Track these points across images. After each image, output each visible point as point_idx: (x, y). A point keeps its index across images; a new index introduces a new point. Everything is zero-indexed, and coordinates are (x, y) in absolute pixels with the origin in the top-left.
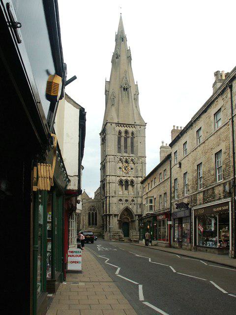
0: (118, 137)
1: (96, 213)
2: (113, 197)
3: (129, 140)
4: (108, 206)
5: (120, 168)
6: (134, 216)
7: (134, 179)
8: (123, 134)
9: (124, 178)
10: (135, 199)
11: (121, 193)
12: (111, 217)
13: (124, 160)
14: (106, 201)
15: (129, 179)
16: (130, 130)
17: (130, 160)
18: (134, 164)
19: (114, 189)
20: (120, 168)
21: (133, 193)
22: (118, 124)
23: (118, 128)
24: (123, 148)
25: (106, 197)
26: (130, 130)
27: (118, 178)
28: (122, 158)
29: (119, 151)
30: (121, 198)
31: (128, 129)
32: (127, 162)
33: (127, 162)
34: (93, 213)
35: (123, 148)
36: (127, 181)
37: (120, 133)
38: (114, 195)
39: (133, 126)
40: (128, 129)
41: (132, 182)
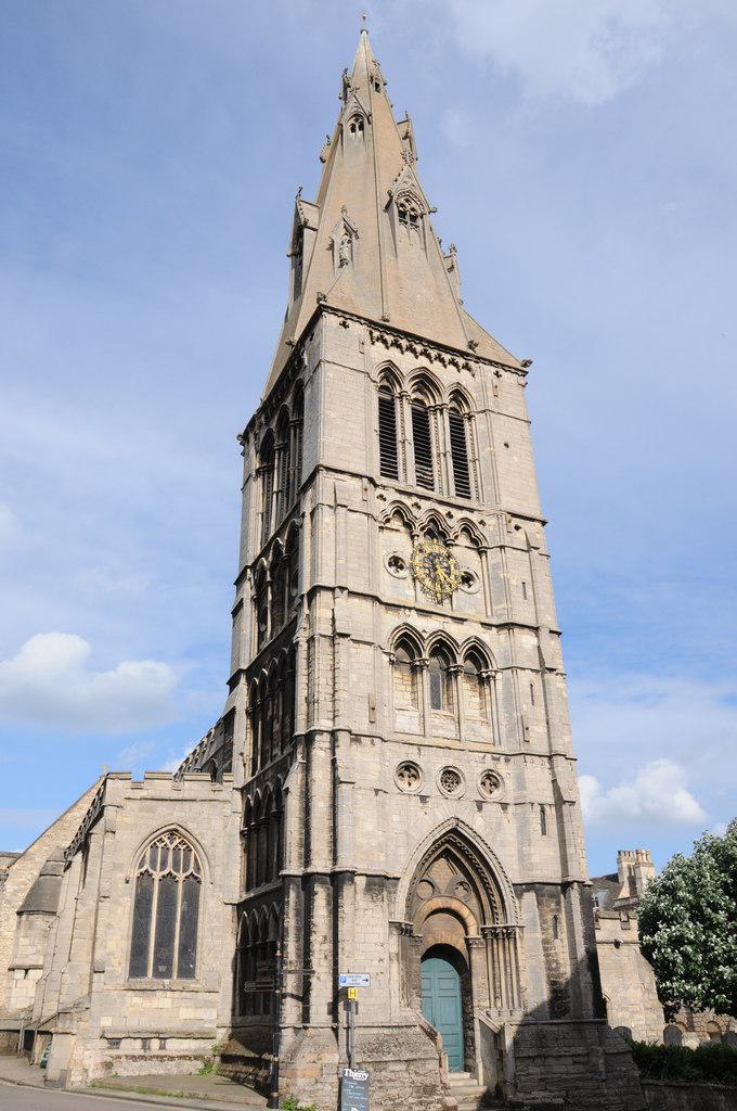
1: (194, 882)
2: (356, 738)
3: (440, 429)
4: (320, 806)
5: (396, 562)
7: (488, 637)
8: (408, 386)
10: (503, 769)
11: (407, 722)
12: (347, 891)
13: (421, 516)
14: (307, 768)
15: (459, 633)
16: (447, 376)
17: (454, 525)
18: (481, 552)
19: (365, 688)
20: (396, 562)
21: (485, 733)
22: (382, 330)
23: (380, 354)
24: (406, 453)
25: (309, 738)
26: (447, 376)
27: (392, 621)
28: (408, 501)
29: (389, 467)
30: (414, 758)
31: (436, 367)
32: (435, 530)
33: (435, 530)
35: (406, 453)
36: (443, 648)
37: (390, 374)
38: (362, 727)
39: (461, 361)
40: (436, 367)
41: (477, 654)
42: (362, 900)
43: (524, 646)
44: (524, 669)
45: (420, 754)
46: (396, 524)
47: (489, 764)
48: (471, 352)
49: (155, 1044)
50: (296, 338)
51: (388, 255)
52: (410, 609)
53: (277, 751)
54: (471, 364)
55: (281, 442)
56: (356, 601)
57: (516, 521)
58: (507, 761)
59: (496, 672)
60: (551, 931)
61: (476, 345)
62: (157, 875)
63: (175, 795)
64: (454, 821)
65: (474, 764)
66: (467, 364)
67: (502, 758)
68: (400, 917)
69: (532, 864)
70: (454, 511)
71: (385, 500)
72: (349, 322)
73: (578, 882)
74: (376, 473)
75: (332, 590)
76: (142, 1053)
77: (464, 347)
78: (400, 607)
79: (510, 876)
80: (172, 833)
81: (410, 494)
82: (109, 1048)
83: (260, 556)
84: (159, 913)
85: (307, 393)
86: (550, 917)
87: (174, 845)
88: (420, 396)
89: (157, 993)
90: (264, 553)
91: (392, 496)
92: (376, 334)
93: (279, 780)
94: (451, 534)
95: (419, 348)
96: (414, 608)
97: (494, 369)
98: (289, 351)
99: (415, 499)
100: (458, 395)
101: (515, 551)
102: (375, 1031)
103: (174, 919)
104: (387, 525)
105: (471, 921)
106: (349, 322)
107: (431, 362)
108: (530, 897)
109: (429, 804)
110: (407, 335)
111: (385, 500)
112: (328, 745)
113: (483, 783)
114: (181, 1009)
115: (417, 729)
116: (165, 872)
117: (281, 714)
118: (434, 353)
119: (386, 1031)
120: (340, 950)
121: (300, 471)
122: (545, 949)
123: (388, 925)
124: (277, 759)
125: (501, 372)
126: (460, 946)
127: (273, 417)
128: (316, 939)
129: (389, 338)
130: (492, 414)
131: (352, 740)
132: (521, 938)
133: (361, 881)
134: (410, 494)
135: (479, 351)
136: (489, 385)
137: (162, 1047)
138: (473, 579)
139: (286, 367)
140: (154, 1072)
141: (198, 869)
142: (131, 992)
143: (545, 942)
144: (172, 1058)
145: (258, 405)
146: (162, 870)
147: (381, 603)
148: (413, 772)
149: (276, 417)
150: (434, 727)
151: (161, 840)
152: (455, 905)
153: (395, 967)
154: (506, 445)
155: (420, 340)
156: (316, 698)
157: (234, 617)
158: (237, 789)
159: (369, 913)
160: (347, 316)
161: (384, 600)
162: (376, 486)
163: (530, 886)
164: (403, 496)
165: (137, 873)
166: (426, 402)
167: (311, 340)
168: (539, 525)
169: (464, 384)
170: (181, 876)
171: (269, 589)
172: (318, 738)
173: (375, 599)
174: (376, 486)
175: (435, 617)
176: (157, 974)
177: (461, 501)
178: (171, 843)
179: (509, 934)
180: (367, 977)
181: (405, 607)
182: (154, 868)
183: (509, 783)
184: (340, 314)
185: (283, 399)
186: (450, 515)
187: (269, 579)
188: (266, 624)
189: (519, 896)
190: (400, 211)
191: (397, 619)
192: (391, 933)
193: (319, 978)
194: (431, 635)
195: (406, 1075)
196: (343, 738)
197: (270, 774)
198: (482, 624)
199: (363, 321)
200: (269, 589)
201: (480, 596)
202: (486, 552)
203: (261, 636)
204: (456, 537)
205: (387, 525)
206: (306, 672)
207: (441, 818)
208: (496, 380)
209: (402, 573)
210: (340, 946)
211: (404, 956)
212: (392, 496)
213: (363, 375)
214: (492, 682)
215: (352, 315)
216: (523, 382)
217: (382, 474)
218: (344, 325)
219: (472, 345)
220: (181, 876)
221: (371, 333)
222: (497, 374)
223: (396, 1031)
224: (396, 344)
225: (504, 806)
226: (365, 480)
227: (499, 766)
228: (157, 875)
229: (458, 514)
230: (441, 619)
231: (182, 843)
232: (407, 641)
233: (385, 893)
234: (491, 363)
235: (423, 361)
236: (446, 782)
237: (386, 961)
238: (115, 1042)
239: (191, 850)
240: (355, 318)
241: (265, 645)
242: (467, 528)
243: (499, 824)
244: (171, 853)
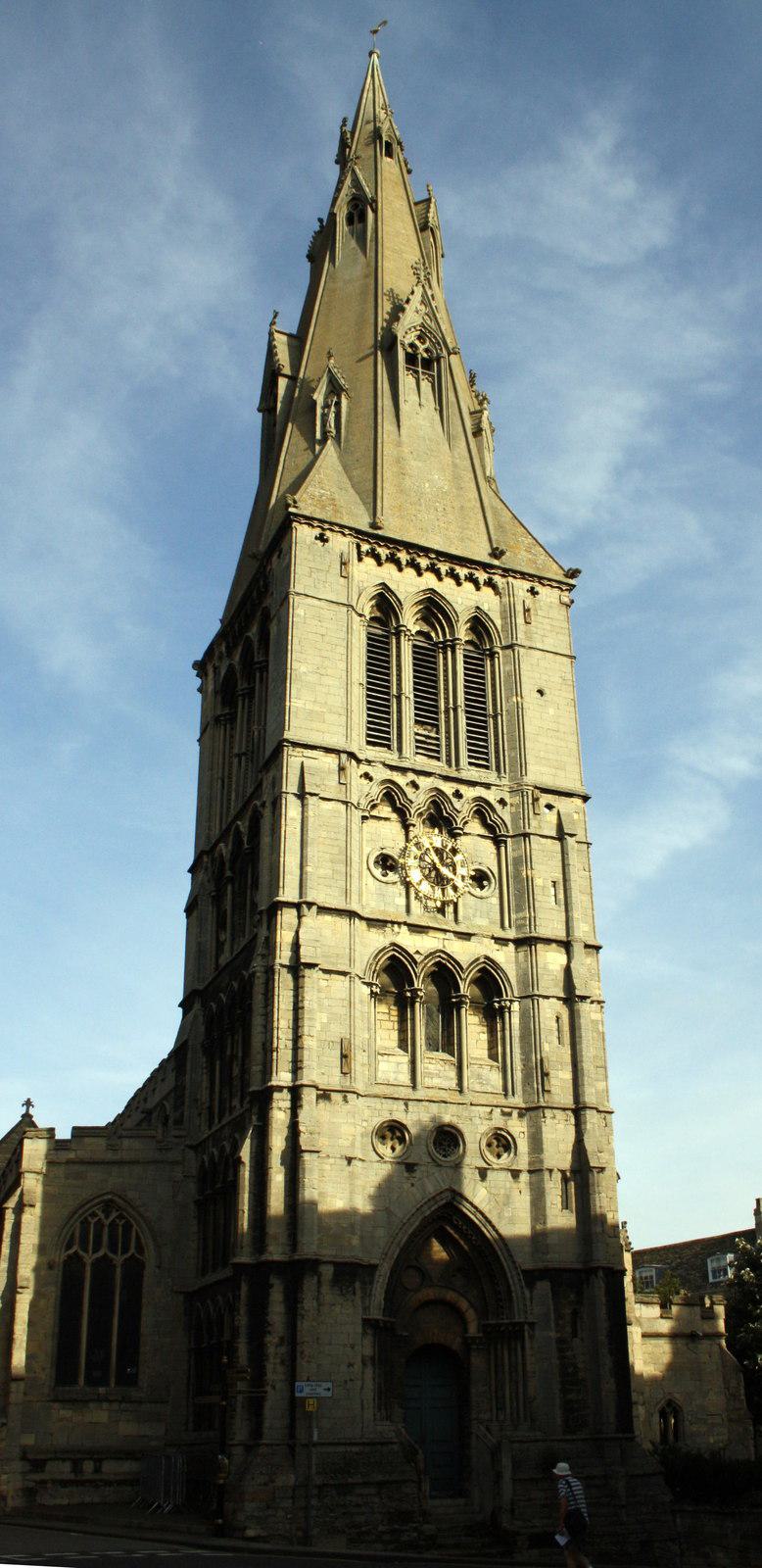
0: (370, 638)
1: (134, 1271)
2: (325, 1095)
5: (386, 862)
6: (515, 1282)
8: (410, 620)
9: (419, 945)
11: (394, 1068)
12: (309, 1284)
13: (419, 800)
15: (464, 953)
16: (463, 599)
17: (463, 808)
18: (498, 841)
19: (338, 1031)
20: (386, 862)
22: (376, 543)
23: (369, 574)
26: (463, 599)
27: (378, 940)
28: (401, 780)
29: (380, 732)
30: (400, 1115)
31: (446, 587)
33: (440, 817)
34: (103, 1267)
36: (444, 973)
37: (386, 604)
38: (332, 1079)
39: (482, 576)
40: (446, 587)
41: (488, 979)
42: (328, 1294)
43: (551, 967)
44: (547, 997)
45: (407, 1111)
46: (385, 810)
47: (498, 1120)
48: (496, 562)
49: (88, 1466)
50: (262, 548)
51: (387, 425)
52: (399, 924)
53: (236, 1102)
54: (497, 579)
55: (245, 685)
56: (328, 918)
57: (545, 799)
58: (521, 1116)
59: (511, 1001)
60: (568, 1329)
61: (502, 553)
62: (89, 1259)
63: (110, 1156)
64: (448, 1194)
65: (477, 1121)
66: (490, 579)
67: (515, 1113)
68: (376, 1314)
69: (547, 1245)
70: (463, 789)
71: (371, 779)
72: (328, 534)
73: (603, 1268)
74: (358, 743)
75: (297, 906)
76: (72, 1477)
77: (482, 554)
78: (386, 922)
79: (519, 1260)
80: (108, 1206)
81: (404, 770)
82: (31, 1471)
83: (218, 842)
84: (92, 1305)
85: (273, 629)
86: (568, 1311)
87: (111, 1219)
88: (426, 628)
89: (91, 1405)
90: (223, 837)
91: (380, 773)
92: (365, 547)
93: (234, 1138)
94: (459, 822)
95: (424, 562)
96: (405, 923)
97: (527, 585)
98: (256, 564)
99: (411, 776)
100: (479, 624)
101: (544, 840)
102: (341, 1449)
103: (112, 1313)
104: (374, 813)
105: (471, 1315)
106: (328, 534)
107: (440, 579)
108: (543, 1287)
109: (418, 1174)
110: (408, 546)
111: (371, 779)
112: (288, 1104)
113: (489, 1145)
114: (121, 1423)
115: (405, 1078)
116: (100, 1254)
117: (240, 1054)
118: (444, 568)
119: (355, 1449)
120: (298, 1354)
121: (264, 752)
122: (560, 1350)
123: (360, 1322)
124: (236, 1114)
125: (538, 588)
126: (456, 1344)
127: (235, 646)
128: (272, 1340)
129: (383, 552)
130: (522, 650)
131: (319, 1097)
132: (531, 1337)
133: (327, 1271)
134: (404, 770)
135: (506, 561)
136: (520, 608)
137: (97, 1470)
138: (487, 878)
139: (251, 583)
140: (87, 1500)
141: (140, 1249)
142: (56, 1405)
143: (560, 1341)
144: (109, 1483)
145: (217, 627)
146: (95, 1251)
147: (361, 918)
148: (398, 1134)
149: (240, 649)
150: (431, 1075)
151: (94, 1215)
152: (450, 1296)
153: (369, 1372)
154: (541, 692)
155: (426, 551)
156: (275, 1045)
157: (188, 917)
158: (191, 1147)
159: (337, 1309)
160: (326, 526)
161: (365, 914)
162: (359, 761)
163: (545, 1273)
164: (395, 773)
165: (63, 1257)
166: (433, 634)
167: (279, 557)
168: (578, 802)
169: (485, 608)
170: (119, 1259)
171: (229, 888)
172: (276, 1095)
173: (352, 914)
174: (359, 761)
175: (432, 933)
176: (91, 1381)
177: (472, 774)
178: (107, 1217)
179: (515, 1334)
180: (329, 1385)
181: (393, 923)
182: (86, 1251)
183: (523, 1145)
184: (316, 524)
185: (247, 628)
186: (458, 795)
187: (228, 873)
188: (225, 931)
189: (530, 1285)
190: (407, 354)
191: (381, 937)
192: (364, 1333)
193: (274, 1388)
194: (426, 957)
195: (377, 1500)
196: (309, 1096)
197: (227, 1132)
198: (493, 938)
199: (347, 532)
200: (229, 888)
201: (495, 901)
202: (505, 842)
203: (220, 946)
204: (466, 823)
205: (374, 813)
206: (261, 1011)
207: (431, 1189)
208: (529, 600)
209: (392, 877)
210: (299, 1348)
211: (381, 1361)
212: (380, 773)
213: (345, 609)
214: (507, 1014)
215: (331, 524)
216: (566, 600)
217: (369, 743)
218: (322, 538)
219: (496, 553)
220: (119, 1259)
221: (358, 547)
222: (533, 592)
223: (367, 1449)
224: (393, 559)
225: (515, 1174)
226: (344, 757)
227: (510, 1123)
228: (89, 1259)
229: (470, 793)
230: (441, 935)
231: (121, 1217)
232: (396, 970)
233: (357, 1285)
234: (524, 575)
235: (429, 580)
236: (441, 1144)
237: (358, 1367)
238: (38, 1465)
239: (132, 1226)
240: (337, 529)
241: (224, 960)
242: (482, 810)
243: (508, 1197)
244: (106, 1230)
